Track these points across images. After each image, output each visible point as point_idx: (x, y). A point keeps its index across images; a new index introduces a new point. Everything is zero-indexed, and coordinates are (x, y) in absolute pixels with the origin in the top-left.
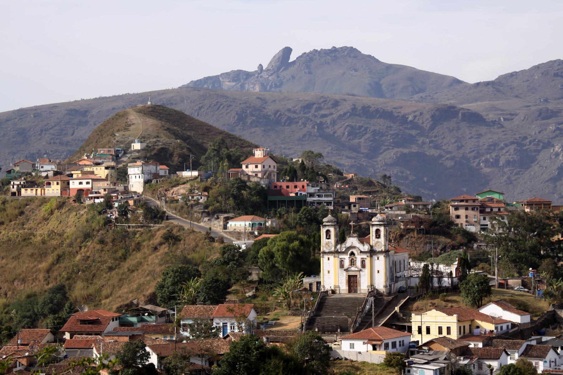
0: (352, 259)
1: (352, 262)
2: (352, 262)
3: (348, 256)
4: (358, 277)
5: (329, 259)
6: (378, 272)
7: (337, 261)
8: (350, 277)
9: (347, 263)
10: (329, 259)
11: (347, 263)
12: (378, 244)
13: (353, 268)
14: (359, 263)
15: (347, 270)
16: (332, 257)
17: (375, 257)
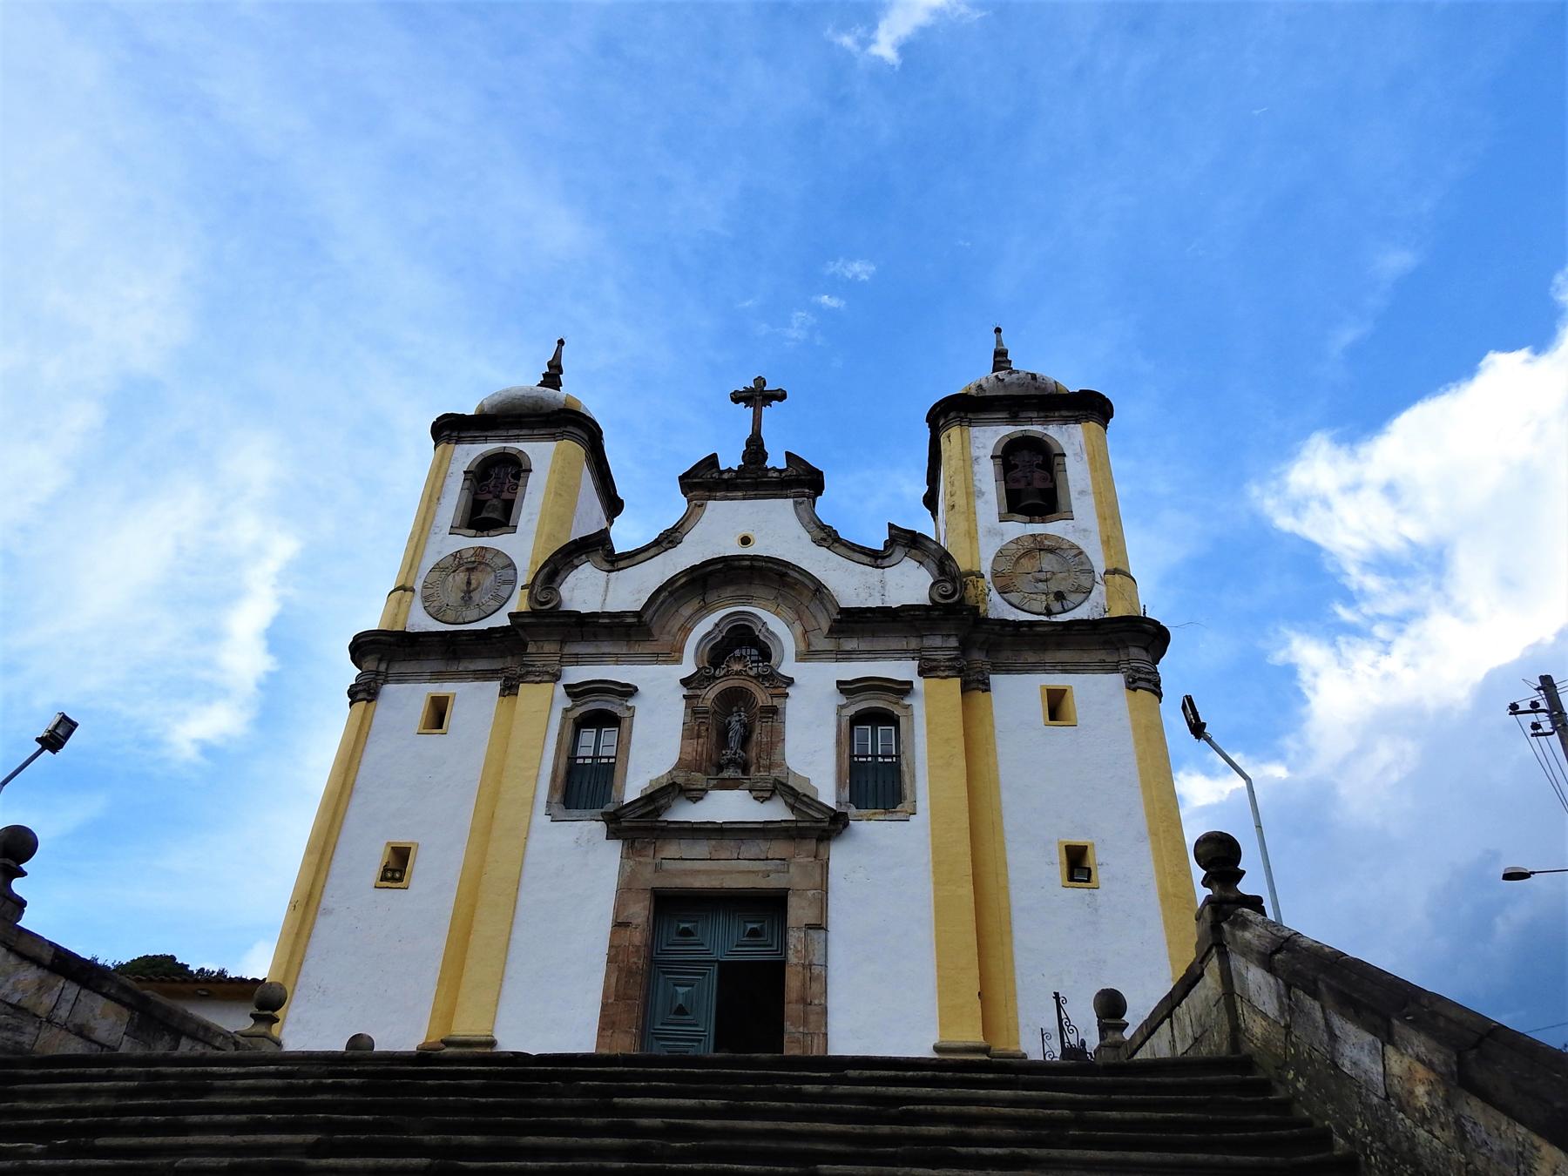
0: (734, 699)
1: (733, 731)
2: (733, 731)
3: (688, 667)
4: (798, 912)
5: (438, 714)
6: (1077, 864)
7: (544, 707)
8: (672, 906)
9: (654, 745)
10: (438, 714)
11: (654, 745)
12: (1048, 562)
13: (729, 805)
14: (811, 747)
15: (638, 826)
16: (474, 700)
17: (1016, 694)
